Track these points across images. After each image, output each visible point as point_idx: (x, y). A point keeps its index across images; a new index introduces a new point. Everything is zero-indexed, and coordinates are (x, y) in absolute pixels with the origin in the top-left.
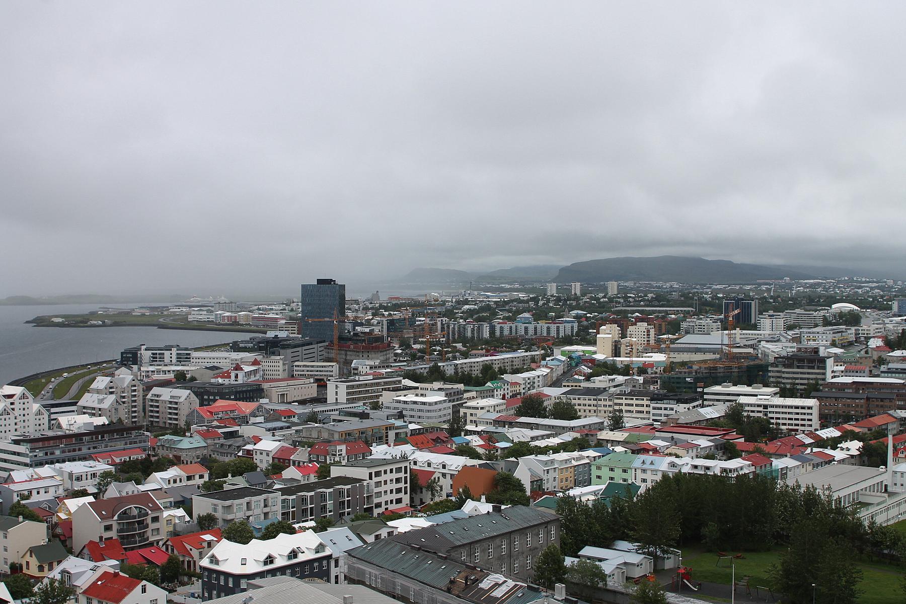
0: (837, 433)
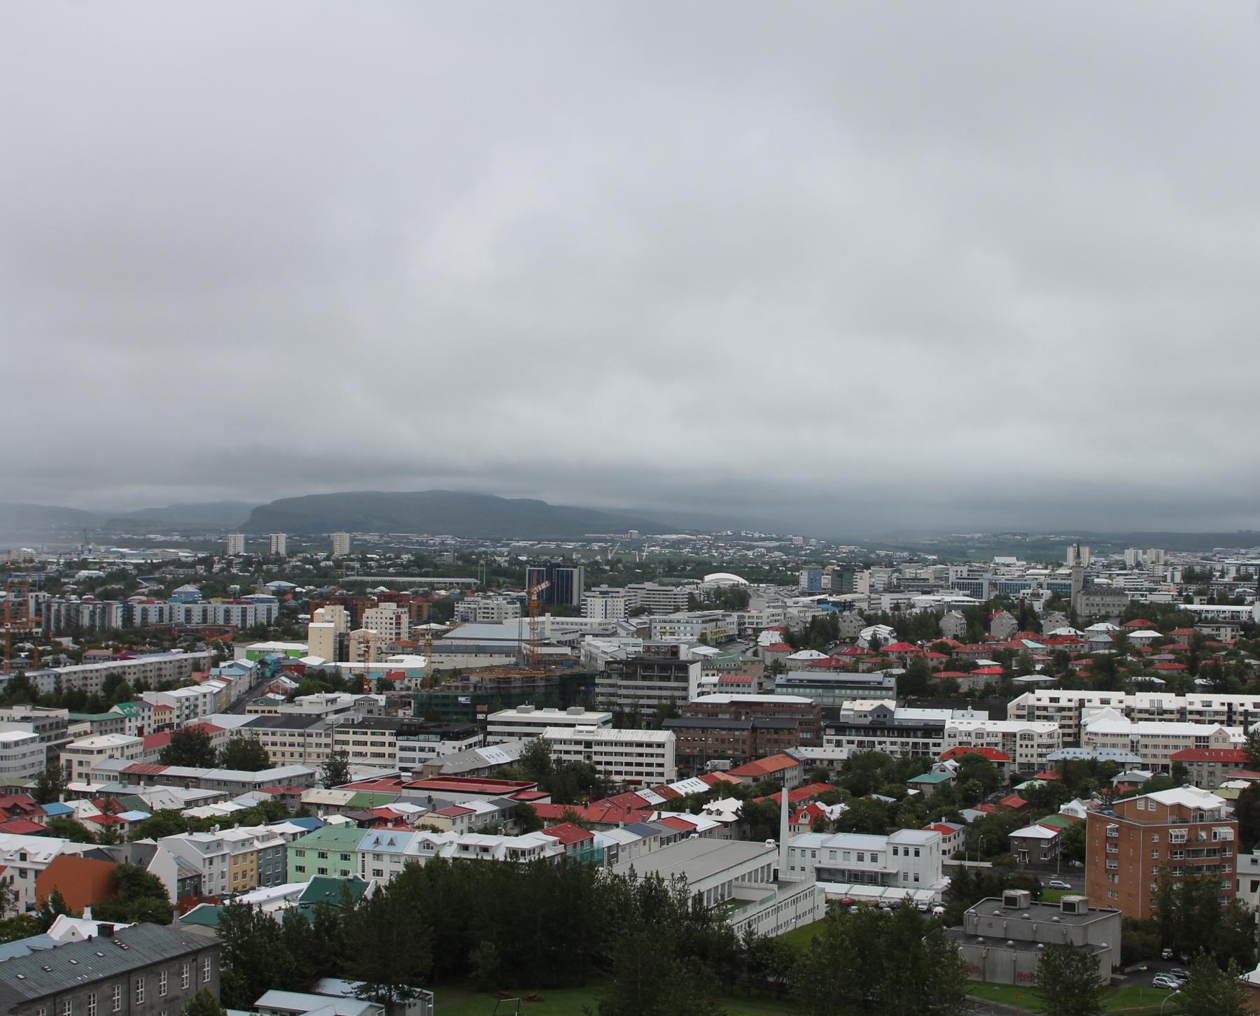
0: (702, 787)
